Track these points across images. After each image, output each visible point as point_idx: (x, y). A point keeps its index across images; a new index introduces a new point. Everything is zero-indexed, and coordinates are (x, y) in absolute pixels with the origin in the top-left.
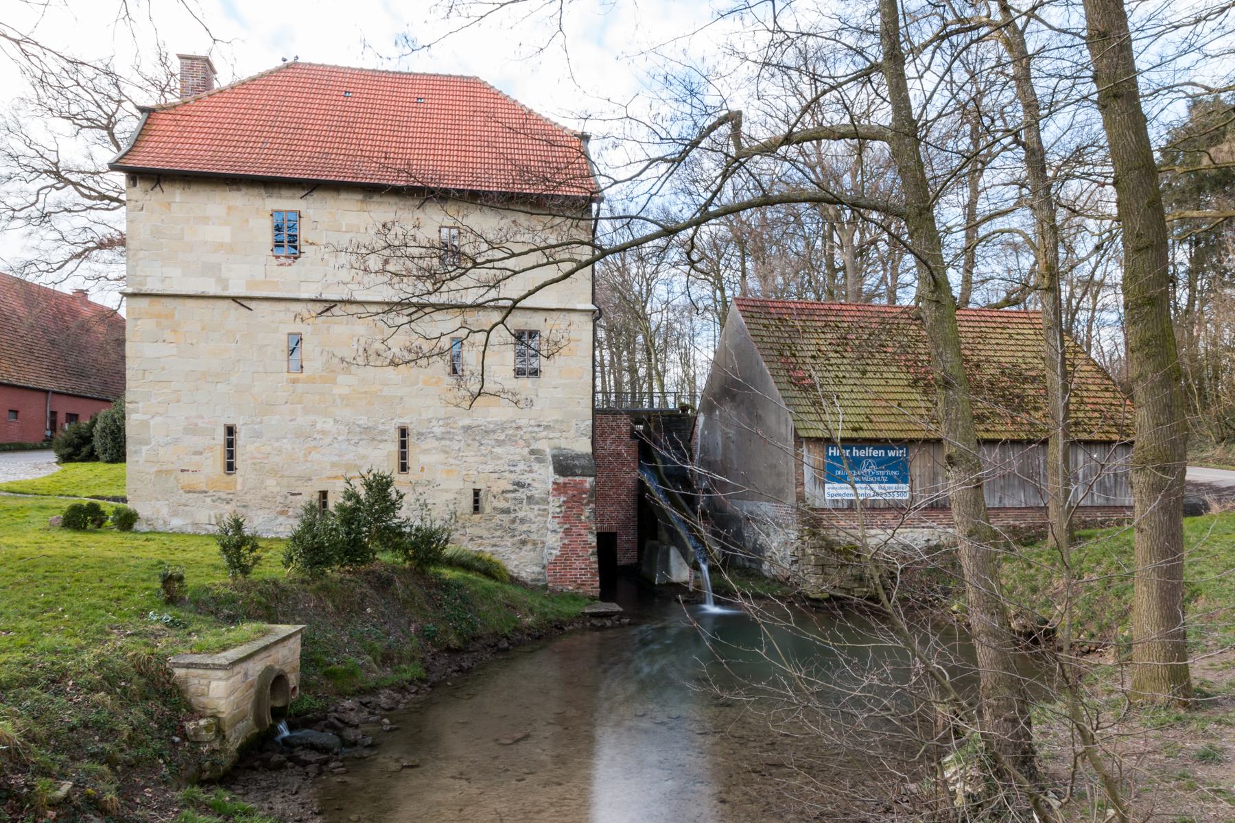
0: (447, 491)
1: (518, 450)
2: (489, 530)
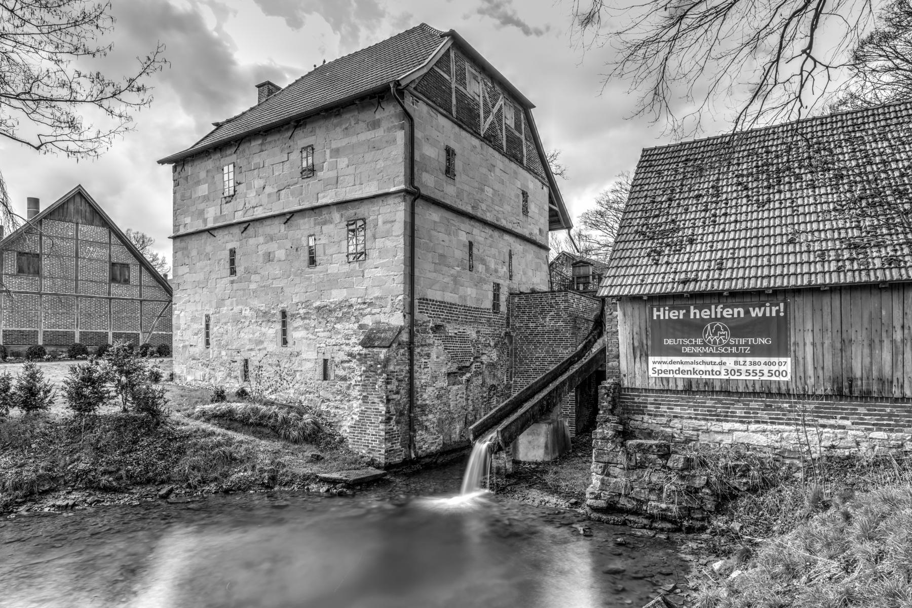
0: (309, 360)
1: (351, 326)
2: (333, 393)
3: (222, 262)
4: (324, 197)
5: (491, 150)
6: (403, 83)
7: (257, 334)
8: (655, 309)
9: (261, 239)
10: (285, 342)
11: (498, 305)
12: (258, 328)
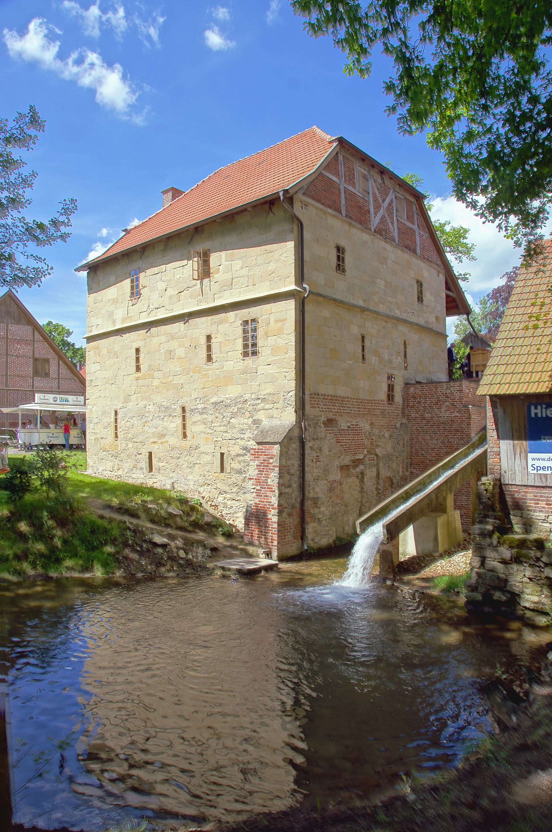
0: (207, 454)
3: (128, 360)
4: (220, 297)
5: (383, 244)
6: (291, 192)
7: (160, 428)
8: (533, 407)
9: (163, 339)
10: (185, 436)
11: (393, 396)
12: (161, 422)
